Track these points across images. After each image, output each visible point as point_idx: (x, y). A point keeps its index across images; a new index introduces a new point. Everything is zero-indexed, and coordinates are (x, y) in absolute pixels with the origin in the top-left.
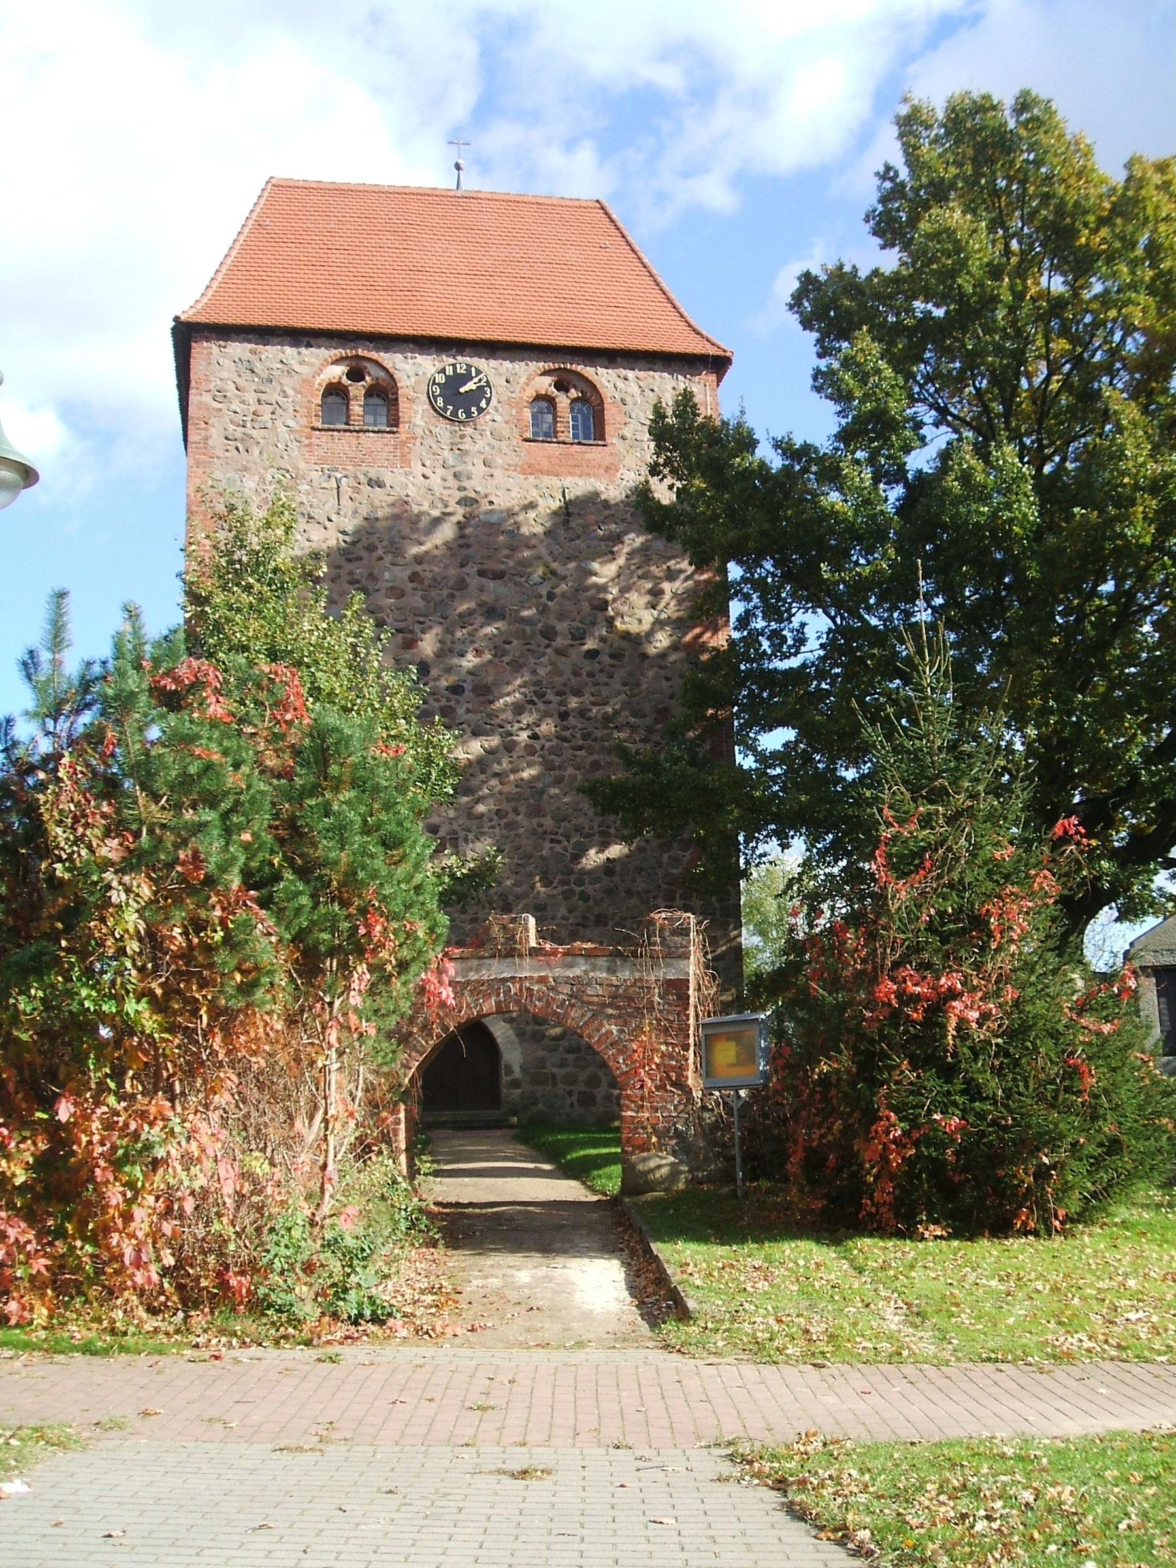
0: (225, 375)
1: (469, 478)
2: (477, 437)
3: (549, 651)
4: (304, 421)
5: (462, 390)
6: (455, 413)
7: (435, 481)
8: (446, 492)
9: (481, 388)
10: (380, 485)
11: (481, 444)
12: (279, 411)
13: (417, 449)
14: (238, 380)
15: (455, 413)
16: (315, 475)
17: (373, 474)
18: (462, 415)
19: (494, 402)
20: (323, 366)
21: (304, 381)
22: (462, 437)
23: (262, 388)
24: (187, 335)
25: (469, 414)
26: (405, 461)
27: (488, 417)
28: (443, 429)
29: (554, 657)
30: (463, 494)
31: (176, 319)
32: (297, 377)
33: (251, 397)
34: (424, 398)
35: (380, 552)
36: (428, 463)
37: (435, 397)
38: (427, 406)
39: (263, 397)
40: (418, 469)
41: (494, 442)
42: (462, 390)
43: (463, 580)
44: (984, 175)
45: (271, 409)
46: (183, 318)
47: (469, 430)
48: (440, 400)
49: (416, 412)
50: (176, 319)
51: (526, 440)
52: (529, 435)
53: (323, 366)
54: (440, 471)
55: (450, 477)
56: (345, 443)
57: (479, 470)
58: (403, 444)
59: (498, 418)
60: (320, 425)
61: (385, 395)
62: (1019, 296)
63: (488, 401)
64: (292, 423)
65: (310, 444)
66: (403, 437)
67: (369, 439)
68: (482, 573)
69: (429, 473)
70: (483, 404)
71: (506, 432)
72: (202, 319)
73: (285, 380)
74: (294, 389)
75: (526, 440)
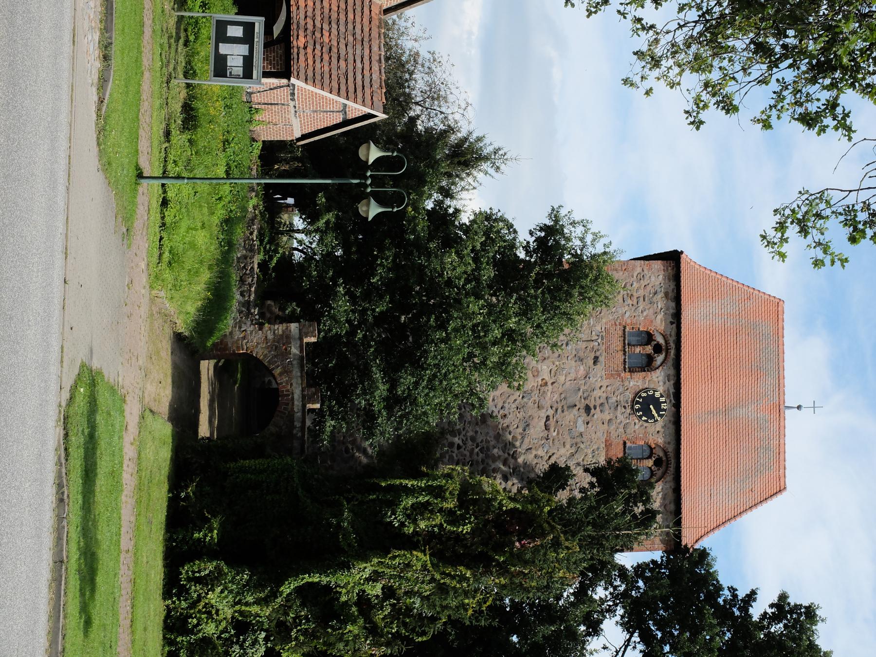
0: (653, 279)
1: (601, 411)
2: (626, 415)
3: (506, 455)
4: (629, 321)
5: (651, 407)
6: (638, 403)
7: (597, 393)
8: (593, 399)
9: (653, 417)
10: (595, 363)
11: (621, 417)
12: (633, 308)
13: (617, 383)
14: (650, 286)
15: (638, 403)
16: (598, 328)
17: (602, 359)
18: (637, 407)
19: (646, 424)
20: (658, 324)
21: (652, 321)
22: (625, 407)
23: (646, 299)
24: (673, 258)
25: (638, 410)
26: (610, 376)
27: (637, 421)
28: (630, 396)
29: (502, 458)
30: (592, 406)
31: (682, 252)
32: (653, 317)
33: (641, 293)
34: (646, 386)
35: (557, 363)
36: (609, 388)
37: (646, 392)
38: (641, 388)
39: (642, 299)
40: (605, 383)
41: (622, 424)
42: (651, 407)
43: (543, 408)
44: (355, 253)
45: (635, 303)
46: (683, 256)
47: (629, 411)
48: (644, 395)
49: (637, 382)
50: (682, 252)
51: (625, 443)
52: (628, 444)
53: (658, 324)
54: (604, 395)
55: (602, 401)
56: (617, 344)
57: (606, 416)
58: (619, 375)
59: (637, 427)
60: (627, 330)
61: (648, 365)
62: (199, 598)
63: (646, 421)
64: (628, 314)
65: (616, 325)
66: (623, 375)
67: (620, 357)
68: (548, 417)
69: (603, 389)
70: (644, 418)
71: (628, 431)
72: (683, 265)
73: (651, 310)
74: (647, 316)
75: (625, 443)
